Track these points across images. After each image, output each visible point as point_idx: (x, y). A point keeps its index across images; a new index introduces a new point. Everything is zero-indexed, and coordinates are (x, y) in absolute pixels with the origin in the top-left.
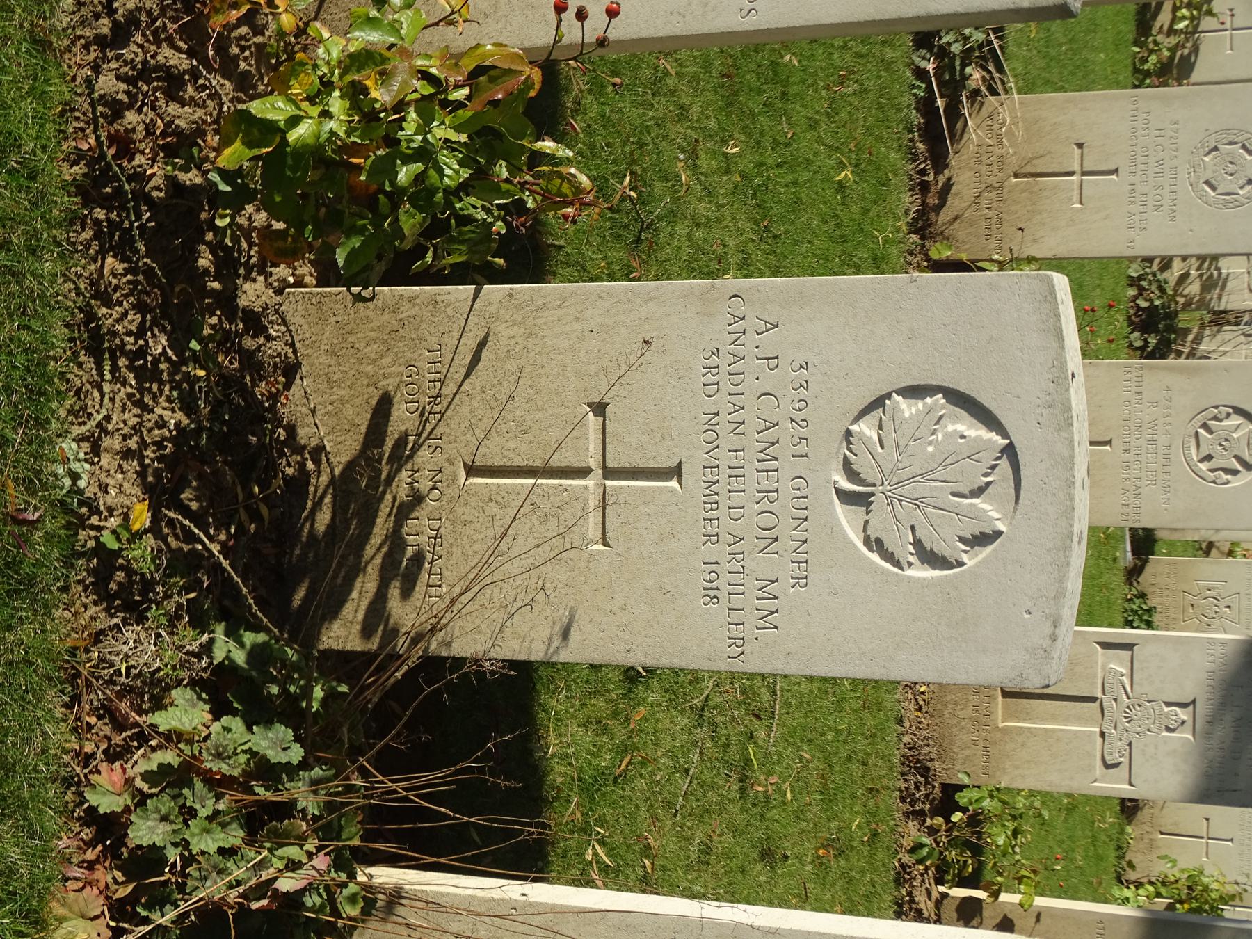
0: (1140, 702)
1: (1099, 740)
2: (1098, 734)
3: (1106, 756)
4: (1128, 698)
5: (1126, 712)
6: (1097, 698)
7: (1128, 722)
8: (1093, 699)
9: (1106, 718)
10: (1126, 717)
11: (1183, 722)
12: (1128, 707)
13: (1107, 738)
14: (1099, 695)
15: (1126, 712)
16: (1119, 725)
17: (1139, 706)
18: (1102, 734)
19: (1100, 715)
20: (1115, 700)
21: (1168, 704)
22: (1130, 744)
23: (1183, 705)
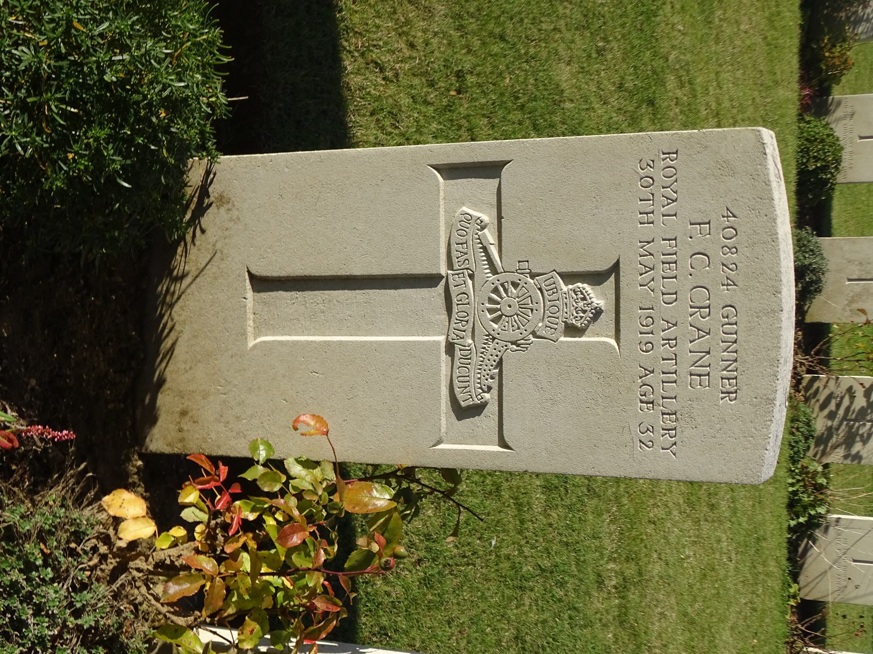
0: (515, 277)
1: (444, 357)
2: (443, 344)
3: (457, 391)
4: (494, 271)
5: (491, 301)
6: (439, 277)
7: (496, 320)
8: (429, 280)
9: (454, 316)
10: (491, 311)
11: (598, 313)
12: (496, 291)
13: (458, 354)
14: (443, 270)
15: (491, 301)
16: (478, 324)
17: (515, 285)
18: (450, 348)
19: (444, 316)
20: (471, 277)
21: (569, 277)
22: (500, 364)
23: (596, 278)
